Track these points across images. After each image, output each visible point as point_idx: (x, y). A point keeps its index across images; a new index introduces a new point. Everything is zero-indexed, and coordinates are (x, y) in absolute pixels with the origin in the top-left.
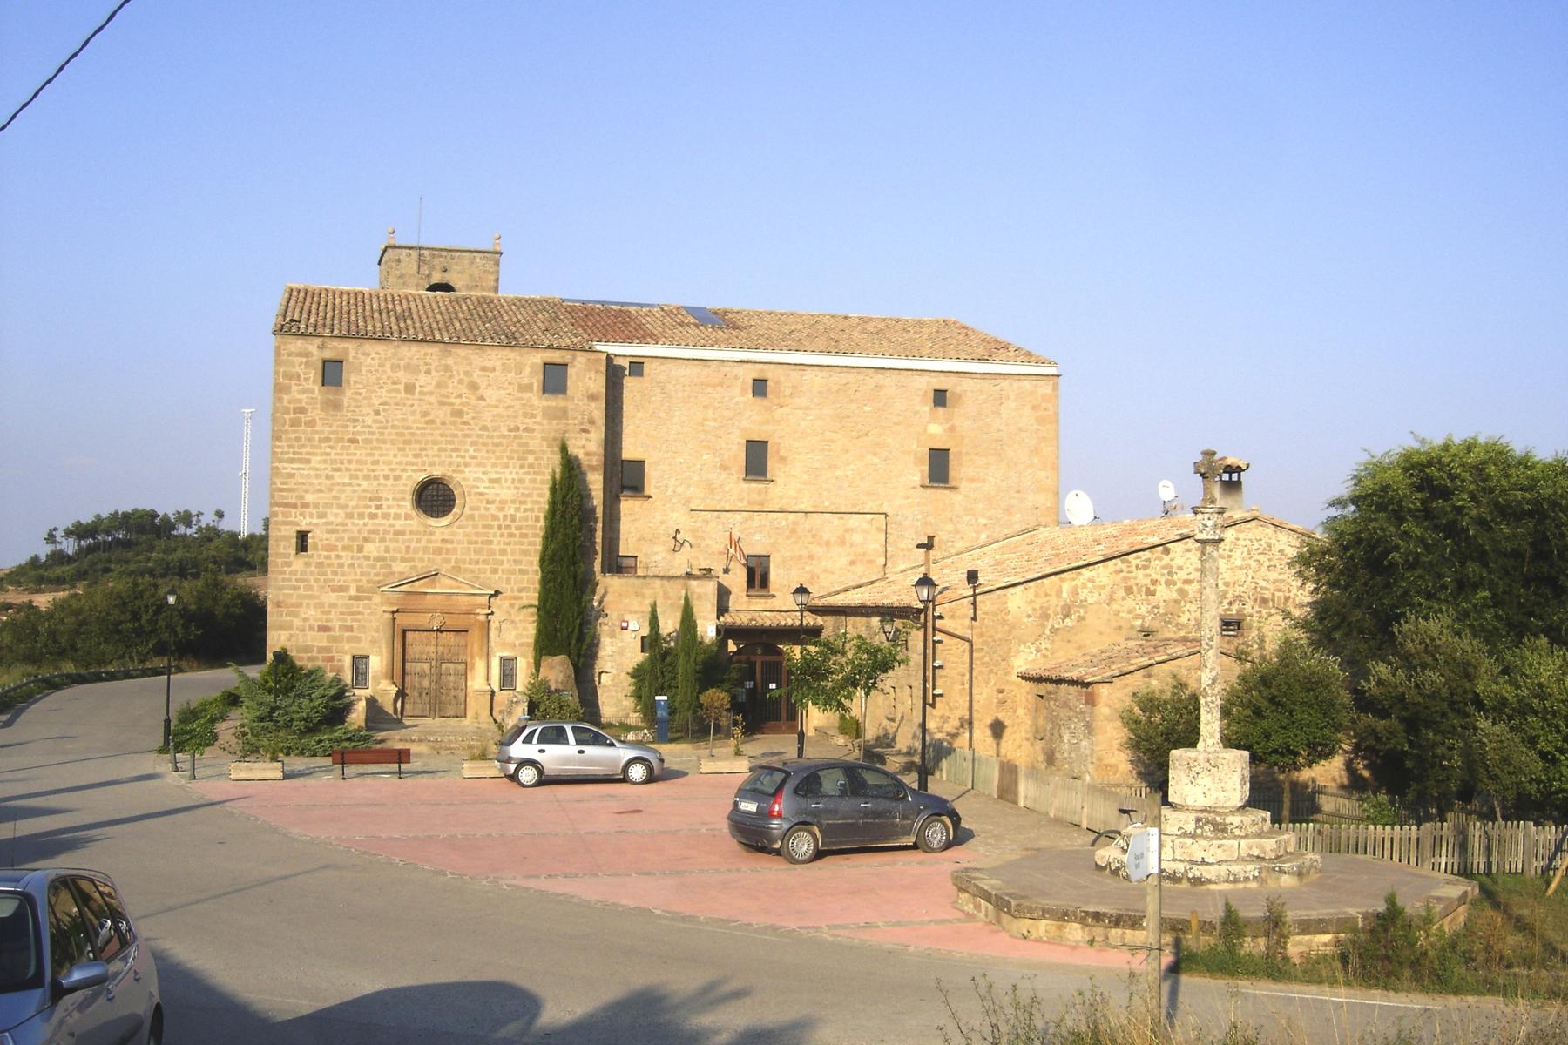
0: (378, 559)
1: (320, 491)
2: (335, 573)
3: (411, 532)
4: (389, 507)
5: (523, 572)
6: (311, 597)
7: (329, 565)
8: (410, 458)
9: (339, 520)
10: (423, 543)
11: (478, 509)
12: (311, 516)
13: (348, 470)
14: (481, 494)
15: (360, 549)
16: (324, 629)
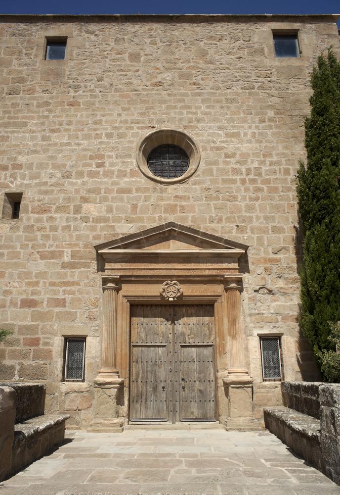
0: (98, 220)
1: (36, 152)
2: (47, 237)
3: (138, 190)
4: (112, 165)
5: (275, 230)
6: (16, 265)
7: (40, 229)
8: (136, 117)
9: (54, 180)
10: (152, 200)
11: (216, 163)
12: (23, 177)
13: (67, 130)
14: (218, 149)
15: (78, 210)
16: (29, 303)
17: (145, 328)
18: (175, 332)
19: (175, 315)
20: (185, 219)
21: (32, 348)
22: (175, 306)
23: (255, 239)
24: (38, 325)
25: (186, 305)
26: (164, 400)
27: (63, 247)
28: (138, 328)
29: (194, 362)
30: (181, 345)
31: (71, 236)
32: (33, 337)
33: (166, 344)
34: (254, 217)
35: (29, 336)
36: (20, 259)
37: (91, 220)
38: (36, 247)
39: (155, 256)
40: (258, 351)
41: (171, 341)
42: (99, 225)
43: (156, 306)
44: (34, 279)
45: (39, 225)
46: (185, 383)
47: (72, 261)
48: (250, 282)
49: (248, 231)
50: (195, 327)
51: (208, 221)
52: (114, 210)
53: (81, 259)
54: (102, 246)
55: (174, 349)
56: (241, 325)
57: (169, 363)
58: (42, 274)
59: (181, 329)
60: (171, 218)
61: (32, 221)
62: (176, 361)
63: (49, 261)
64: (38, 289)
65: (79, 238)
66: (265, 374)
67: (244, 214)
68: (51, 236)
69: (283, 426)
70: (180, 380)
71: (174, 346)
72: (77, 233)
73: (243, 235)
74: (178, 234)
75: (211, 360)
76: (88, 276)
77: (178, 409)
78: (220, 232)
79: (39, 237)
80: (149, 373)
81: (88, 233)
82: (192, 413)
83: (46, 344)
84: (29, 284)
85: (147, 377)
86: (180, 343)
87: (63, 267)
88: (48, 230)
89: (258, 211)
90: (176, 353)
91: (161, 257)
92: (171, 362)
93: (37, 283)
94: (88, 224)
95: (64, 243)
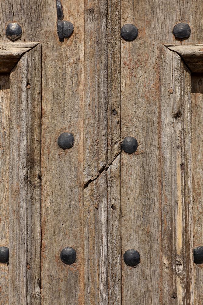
30: (188, 61)
33: (13, 48)
41: (75, 18)
57: (51, 268)
62: (132, 245)
86: (181, 35)
90: (130, 148)
92: (68, 258)
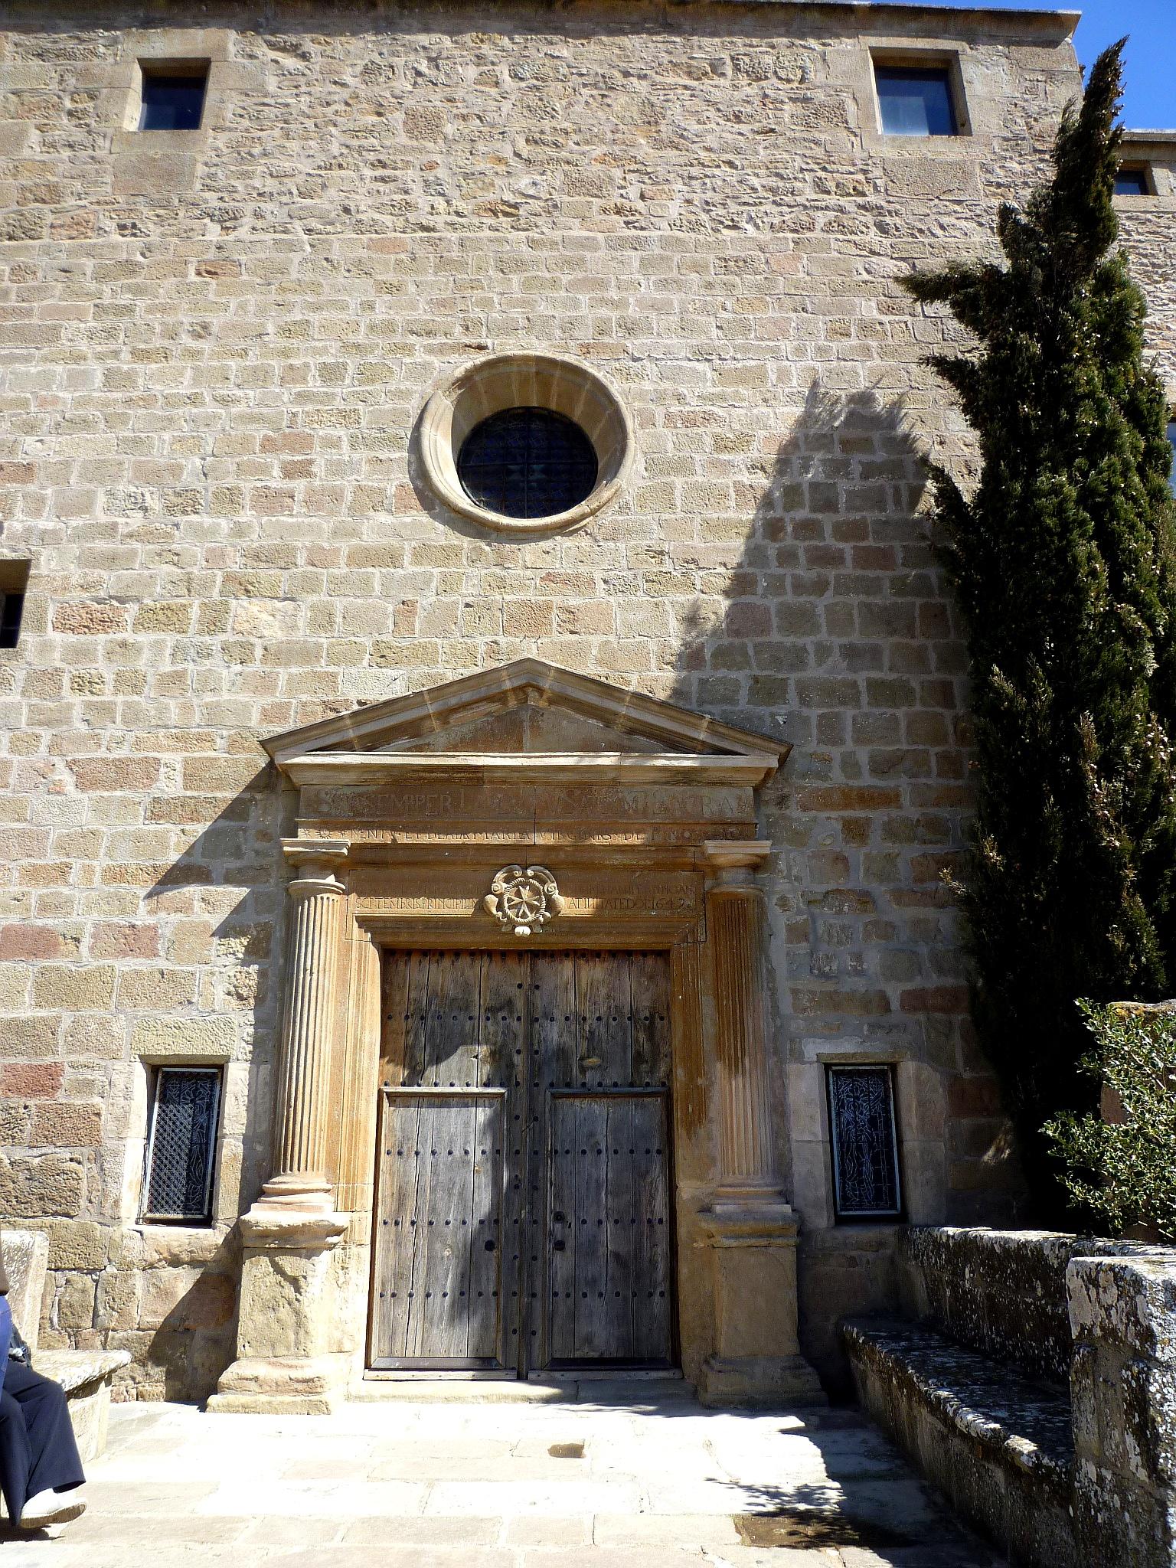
0: (276, 655)
1: (85, 424)
3: (418, 556)
4: (337, 469)
8: (422, 313)
9: (136, 520)
10: (469, 590)
11: (682, 467)
12: (36, 505)
13: (196, 354)
14: (689, 422)
15: (214, 622)
17: (433, 1032)
18: (536, 1047)
19: (537, 987)
20: (580, 652)
21: (31, 1102)
22: (536, 955)
23: (814, 722)
24: (58, 1019)
25: (575, 952)
26: (492, 1290)
27: (159, 747)
28: (408, 1032)
29: (599, 1152)
31: (186, 709)
32: (36, 1062)
34: (811, 648)
35: (22, 1060)
36: (6, 786)
37: (259, 652)
38: (65, 745)
39: (471, 779)
40: (818, 1117)
42: (283, 674)
43: (473, 954)
44: (53, 858)
45: (81, 669)
46: (567, 1230)
47: (189, 793)
48: (795, 871)
49: (792, 694)
50: (603, 1030)
51: (653, 662)
52: (339, 619)
53: (217, 788)
54: (287, 740)
55: (531, 1110)
56: (760, 1024)
58: (83, 842)
59: (556, 1037)
60: (530, 650)
61: (57, 655)
63: (106, 794)
64: (65, 890)
65: (213, 714)
66: (844, 1197)
67: (775, 637)
68: (119, 709)
69: (909, 1400)
70: (549, 1217)
71: (532, 1097)
72: (209, 698)
73: (773, 709)
74: (551, 702)
75: (656, 1145)
76: (238, 847)
77: (538, 1325)
78: (694, 700)
79: (77, 713)
80: (440, 1194)
81: (243, 697)
82: (589, 1340)
83: (87, 1086)
84: (33, 875)
85: (433, 1209)
87: (154, 816)
88: (109, 688)
89: (824, 629)
91: (491, 782)
93: (64, 870)
94: (249, 669)
95: (162, 732)
